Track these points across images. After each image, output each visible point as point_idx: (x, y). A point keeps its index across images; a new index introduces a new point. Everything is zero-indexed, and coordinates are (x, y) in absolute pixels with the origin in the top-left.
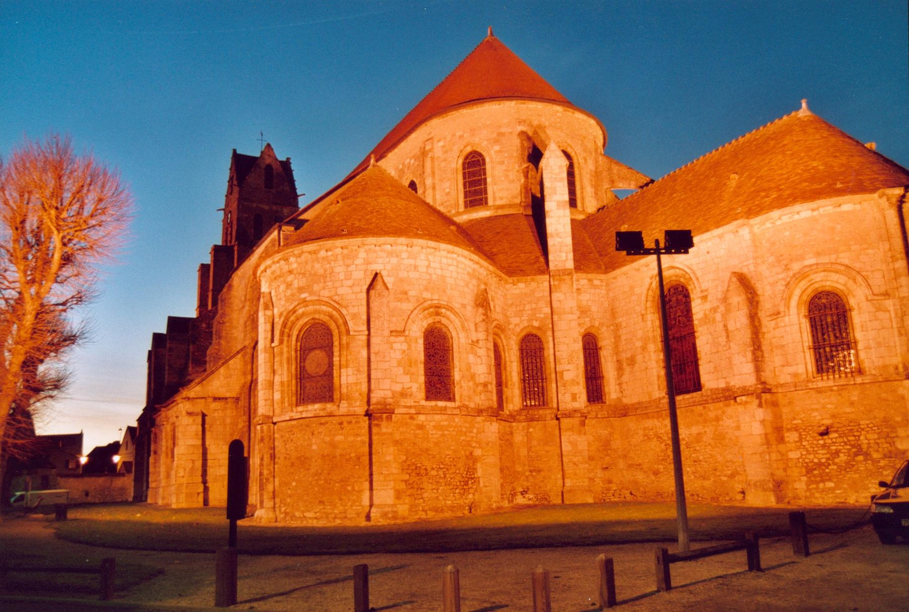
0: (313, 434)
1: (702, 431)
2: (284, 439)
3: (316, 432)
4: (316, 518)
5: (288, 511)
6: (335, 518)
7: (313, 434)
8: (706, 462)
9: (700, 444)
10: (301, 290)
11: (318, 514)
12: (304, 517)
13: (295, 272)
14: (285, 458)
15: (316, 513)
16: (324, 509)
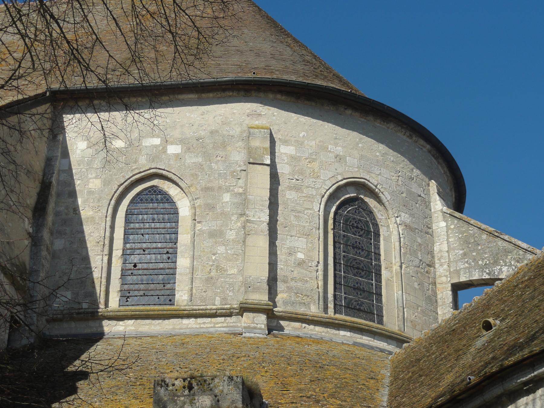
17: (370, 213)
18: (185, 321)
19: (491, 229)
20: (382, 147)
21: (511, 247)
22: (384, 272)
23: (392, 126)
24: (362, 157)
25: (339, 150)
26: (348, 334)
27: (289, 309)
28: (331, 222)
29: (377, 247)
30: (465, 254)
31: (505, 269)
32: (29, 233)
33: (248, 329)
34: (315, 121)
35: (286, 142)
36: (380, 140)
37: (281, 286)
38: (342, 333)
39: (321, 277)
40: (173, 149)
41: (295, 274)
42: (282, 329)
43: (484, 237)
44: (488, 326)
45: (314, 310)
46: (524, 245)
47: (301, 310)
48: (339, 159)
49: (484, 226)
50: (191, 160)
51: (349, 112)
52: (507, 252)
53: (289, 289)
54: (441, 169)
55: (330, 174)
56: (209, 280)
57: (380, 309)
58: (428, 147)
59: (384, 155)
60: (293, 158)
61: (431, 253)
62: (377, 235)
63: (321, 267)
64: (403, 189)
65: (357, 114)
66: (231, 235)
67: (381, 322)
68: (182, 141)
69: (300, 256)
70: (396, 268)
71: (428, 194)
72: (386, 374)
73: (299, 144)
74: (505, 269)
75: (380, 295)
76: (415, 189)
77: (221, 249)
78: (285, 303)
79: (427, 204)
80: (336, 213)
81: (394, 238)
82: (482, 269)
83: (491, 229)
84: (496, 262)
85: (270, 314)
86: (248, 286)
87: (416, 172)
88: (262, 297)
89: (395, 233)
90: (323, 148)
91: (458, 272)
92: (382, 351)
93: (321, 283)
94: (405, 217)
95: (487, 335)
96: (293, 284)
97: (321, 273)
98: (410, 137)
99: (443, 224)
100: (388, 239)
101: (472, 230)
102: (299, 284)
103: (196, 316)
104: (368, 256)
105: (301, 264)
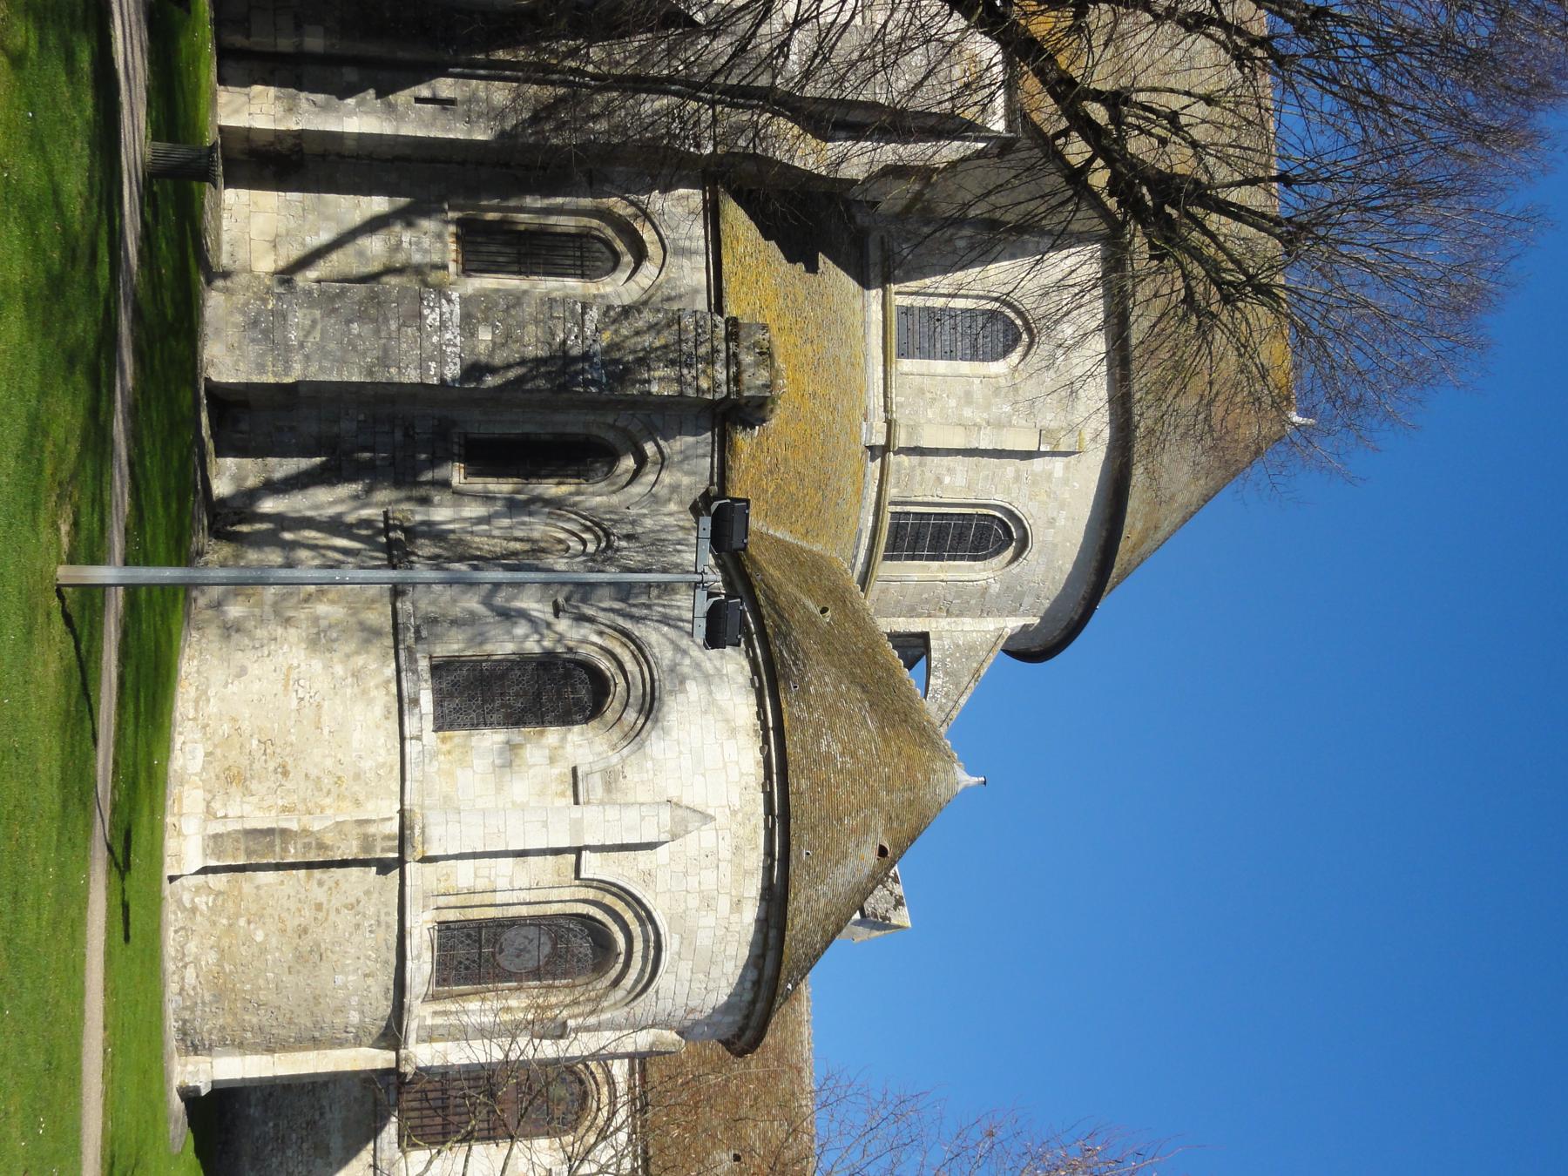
0: (366, 976)
1: (331, 1159)
2: (364, 899)
3: (370, 981)
4: (182, 989)
5: (199, 918)
6: (185, 1022)
7: (366, 976)
8: (281, 1163)
9: (311, 1151)
10: (687, 937)
11: (192, 993)
12: (185, 967)
13: (735, 918)
14: (319, 907)
15: (194, 988)
16: (204, 1003)
17: (997, 552)
18: (880, 369)
19: (982, 673)
20: (1069, 567)
21: (962, 689)
22: (937, 563)
23: (1093, 578)
24: (1055, 545)
25: (1061, 522)
26: (870, 524)
27: (893, 468)
28: (985, 511)
29: (962, 558)
30: (958, 646)
31: (940, 681)
33: (870, 428)
34: (1092, 498)
35: (1067, 468)
36: (1076, 565)
37: (915, 459)
38: (871, 518)
39: (926, 499)
41: (928, 474)
42: (873, 459)
43: (975, 665)
44: (824, 611)
45: (892, 492)
46: (963, 701)
47: (892, 479)
48: (1051, 522)
49: (986, 666)
51: (1104, 534)
52: (957, 685)
53: (913, 468)
54: (1056, 633)
55: (1034, 512)
56: (921, 391)
57: (898, 558)
58: (1076, 617)
59: (1060, 568)
60: (1049, 476)
61: (960, 615)
62: (975, 559)
63: (937, 500)
64: (1025, 588)
65: (1101, 542)
66: (968, 413)
67: (886, 558)
69: (947, 480)
70: (942, 576)
71: (1024, 615)
72: (817, 548)
73: (1066, 481)
74: (940, 681)
75: (913, 558)
76: (1028, 601)
77: (953, 403)
78: (899, 464)
79: (1013, 612)
80: (994, 517)
81: (973, 576)
82: (943, 661)
83: (982, 673)
84: (946, 674)
85: (885, 449)
86: (913, 429)
87: (1047, 604)
88: (902, 440)
89: (978, 577)
90: (1062, 505)
91: (940, 638)
92: (855, 557)
93: (920, 499)
94: (995, 588)
95: (817, 611)
96: (918, 472)
97: (930, 499)
98: (1084, 598)
99: (992, 627)
100: (971, 569)
101: (983, 654)
102: (918, 478)
103: (885, 379)
104: (952, 548)
105: (939, 480)
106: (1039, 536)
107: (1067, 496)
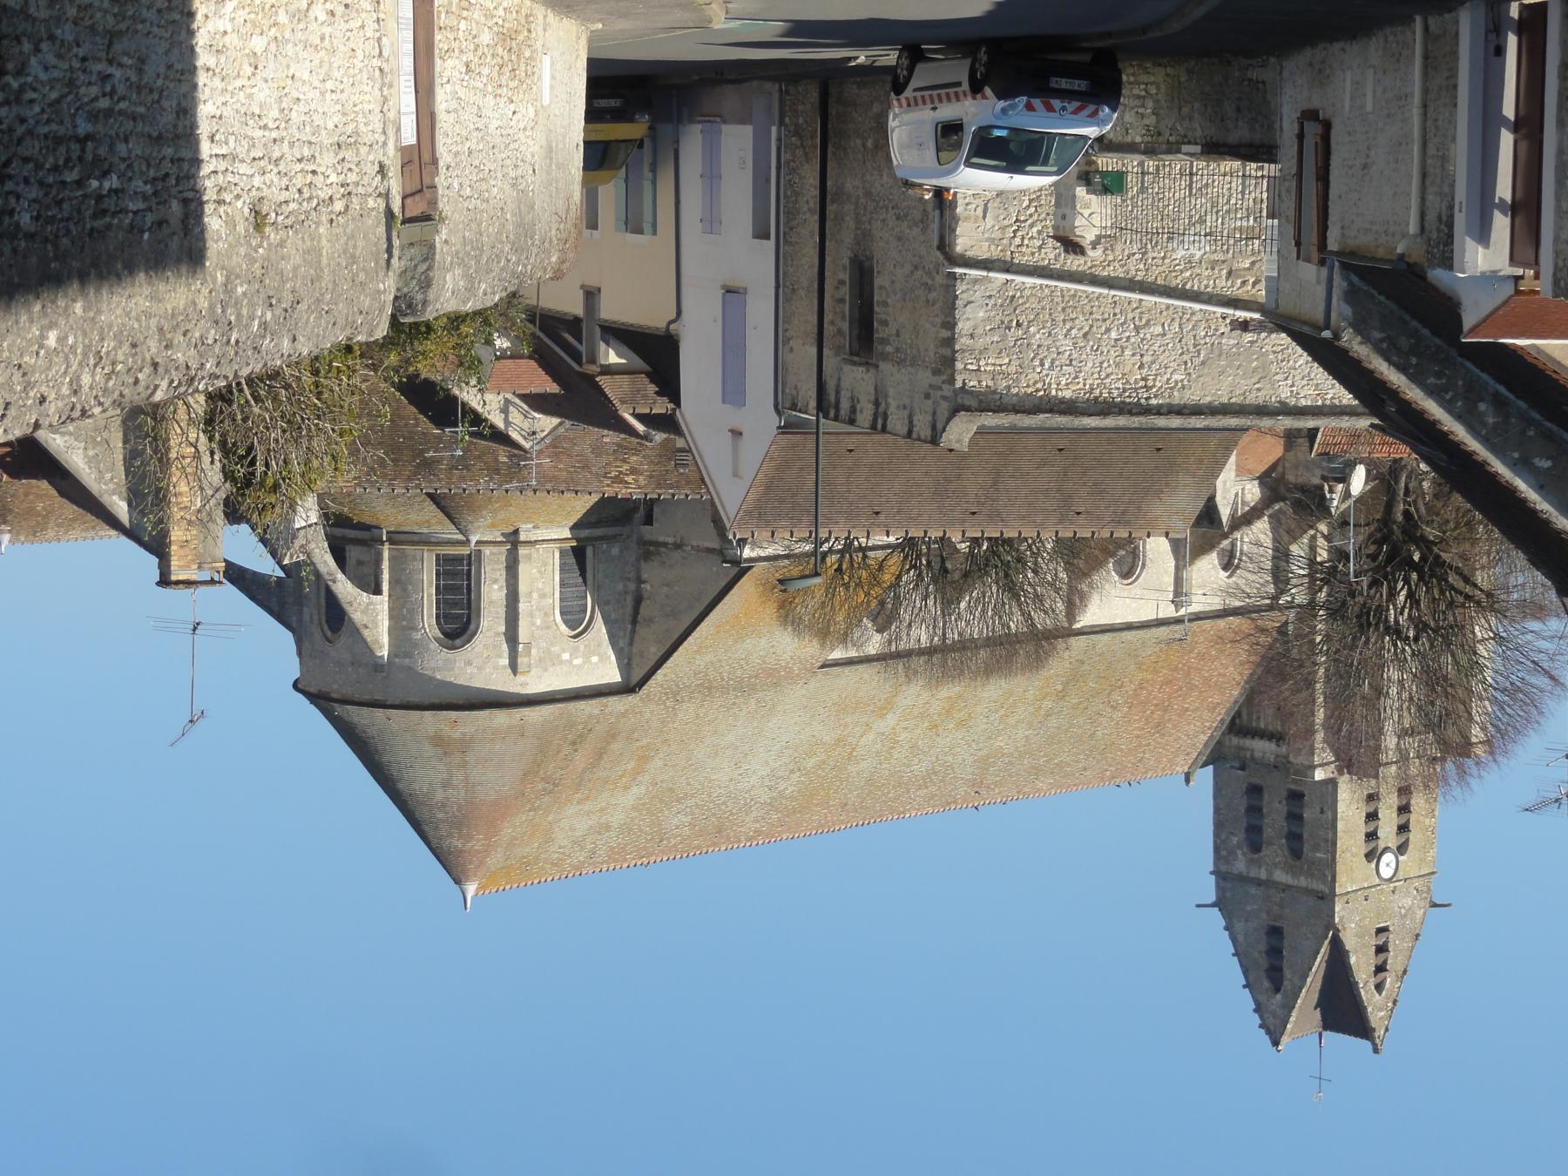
18: (556, 537)
29: (438, 608)
32: (644, 582)
35: (504, 667)
40: (566, 656)
48: (469, 663)
50: (556, 649)
56: (545, 565)
60: (500, 656)
66: (535, 595)
68: (562, 662)
69: (496, 587)
73: (496, 668)
75: (438, 574)
77: (540, 586)
86: (529, 557)
90: (480, 668)
94: (417, 636)
98: (408, 702)
100: (430, 616)
102: (496, 567)
103: (551, 540)
106: (460, 656)
107: (488, 670)
